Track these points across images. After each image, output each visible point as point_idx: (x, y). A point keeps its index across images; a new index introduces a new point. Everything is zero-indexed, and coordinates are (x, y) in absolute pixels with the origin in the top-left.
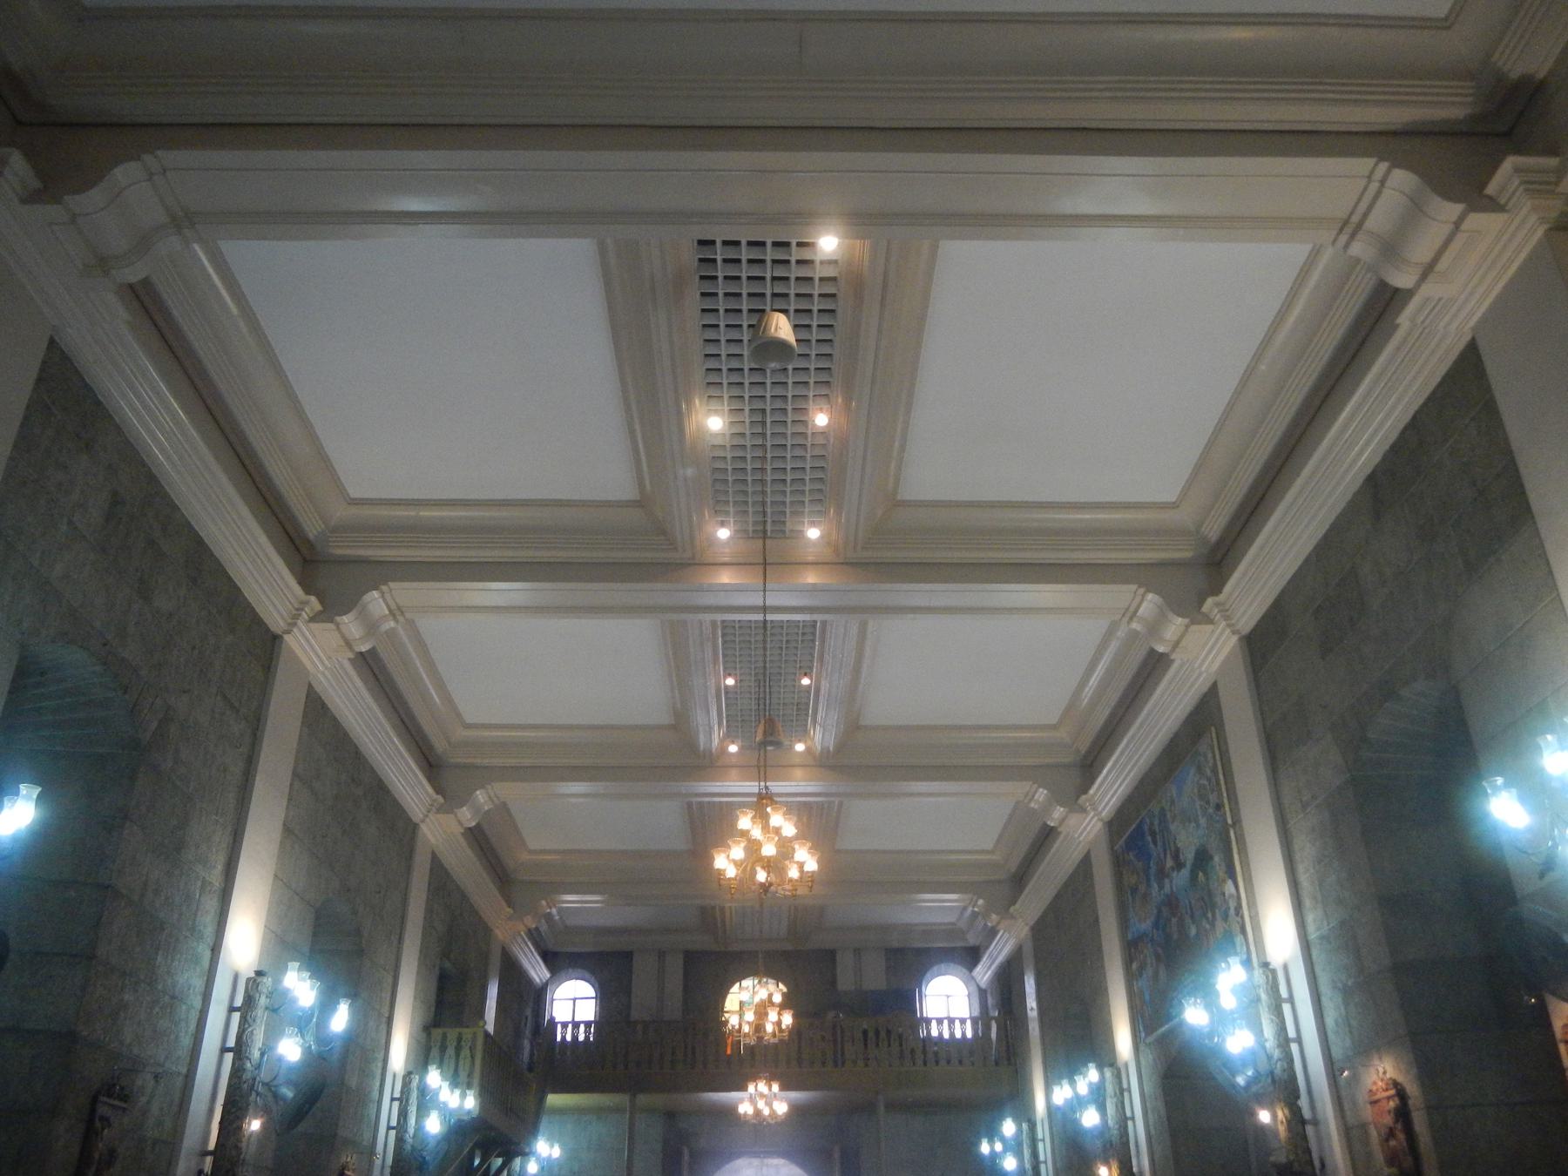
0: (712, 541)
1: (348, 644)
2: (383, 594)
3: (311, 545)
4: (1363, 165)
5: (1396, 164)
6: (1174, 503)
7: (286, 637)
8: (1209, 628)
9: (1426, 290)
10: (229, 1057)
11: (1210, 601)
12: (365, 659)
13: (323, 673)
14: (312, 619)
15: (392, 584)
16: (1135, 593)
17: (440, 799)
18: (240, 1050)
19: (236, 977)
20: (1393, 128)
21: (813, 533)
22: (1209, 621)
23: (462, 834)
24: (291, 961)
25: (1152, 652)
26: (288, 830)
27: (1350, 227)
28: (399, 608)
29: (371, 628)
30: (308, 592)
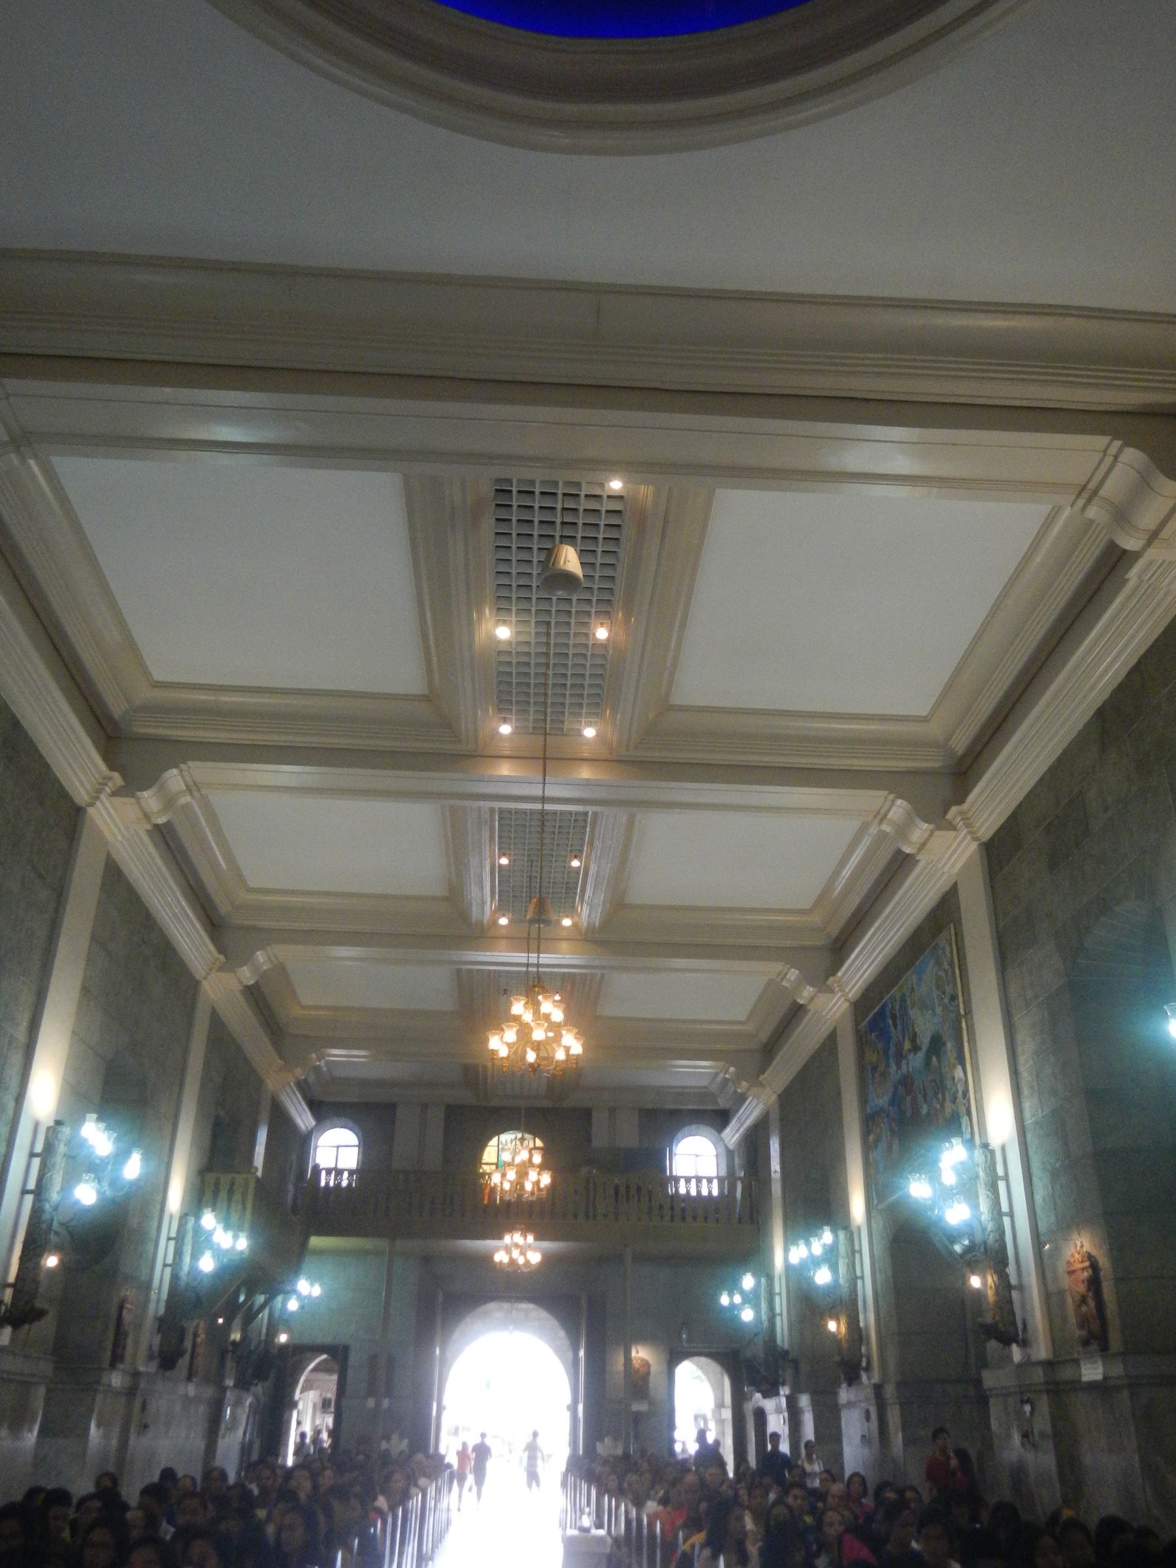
0: (495, 734)
1: (147, 816)
2: (181, 771)
3: (114, 723)
4: (1101, 441)
5: (1127, 444)
6: (926, 717)
7: (90, 810)
8: (952, 834)
9: (1151, 554)
10: (29, 1199)
11: (954, 809)
12: (162, 833)
13: (121, 842)
14: (114, 794)
15: (190, 764)
16: (886, 798)
17: (222, 957)
18: (39, 1192)
19: (37, 1126)
20: (1130, 409)
21: (590, 732)
22: (954, 828)
23: (241, 991)
24: (90, 1113)
25: (899, 852)
26: (85, 990)
27: (1088, 492)
28: (195, 784)
29: (169, 802)
30: (111, 768)
